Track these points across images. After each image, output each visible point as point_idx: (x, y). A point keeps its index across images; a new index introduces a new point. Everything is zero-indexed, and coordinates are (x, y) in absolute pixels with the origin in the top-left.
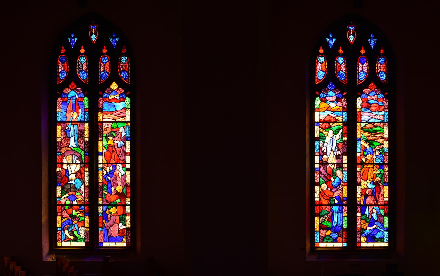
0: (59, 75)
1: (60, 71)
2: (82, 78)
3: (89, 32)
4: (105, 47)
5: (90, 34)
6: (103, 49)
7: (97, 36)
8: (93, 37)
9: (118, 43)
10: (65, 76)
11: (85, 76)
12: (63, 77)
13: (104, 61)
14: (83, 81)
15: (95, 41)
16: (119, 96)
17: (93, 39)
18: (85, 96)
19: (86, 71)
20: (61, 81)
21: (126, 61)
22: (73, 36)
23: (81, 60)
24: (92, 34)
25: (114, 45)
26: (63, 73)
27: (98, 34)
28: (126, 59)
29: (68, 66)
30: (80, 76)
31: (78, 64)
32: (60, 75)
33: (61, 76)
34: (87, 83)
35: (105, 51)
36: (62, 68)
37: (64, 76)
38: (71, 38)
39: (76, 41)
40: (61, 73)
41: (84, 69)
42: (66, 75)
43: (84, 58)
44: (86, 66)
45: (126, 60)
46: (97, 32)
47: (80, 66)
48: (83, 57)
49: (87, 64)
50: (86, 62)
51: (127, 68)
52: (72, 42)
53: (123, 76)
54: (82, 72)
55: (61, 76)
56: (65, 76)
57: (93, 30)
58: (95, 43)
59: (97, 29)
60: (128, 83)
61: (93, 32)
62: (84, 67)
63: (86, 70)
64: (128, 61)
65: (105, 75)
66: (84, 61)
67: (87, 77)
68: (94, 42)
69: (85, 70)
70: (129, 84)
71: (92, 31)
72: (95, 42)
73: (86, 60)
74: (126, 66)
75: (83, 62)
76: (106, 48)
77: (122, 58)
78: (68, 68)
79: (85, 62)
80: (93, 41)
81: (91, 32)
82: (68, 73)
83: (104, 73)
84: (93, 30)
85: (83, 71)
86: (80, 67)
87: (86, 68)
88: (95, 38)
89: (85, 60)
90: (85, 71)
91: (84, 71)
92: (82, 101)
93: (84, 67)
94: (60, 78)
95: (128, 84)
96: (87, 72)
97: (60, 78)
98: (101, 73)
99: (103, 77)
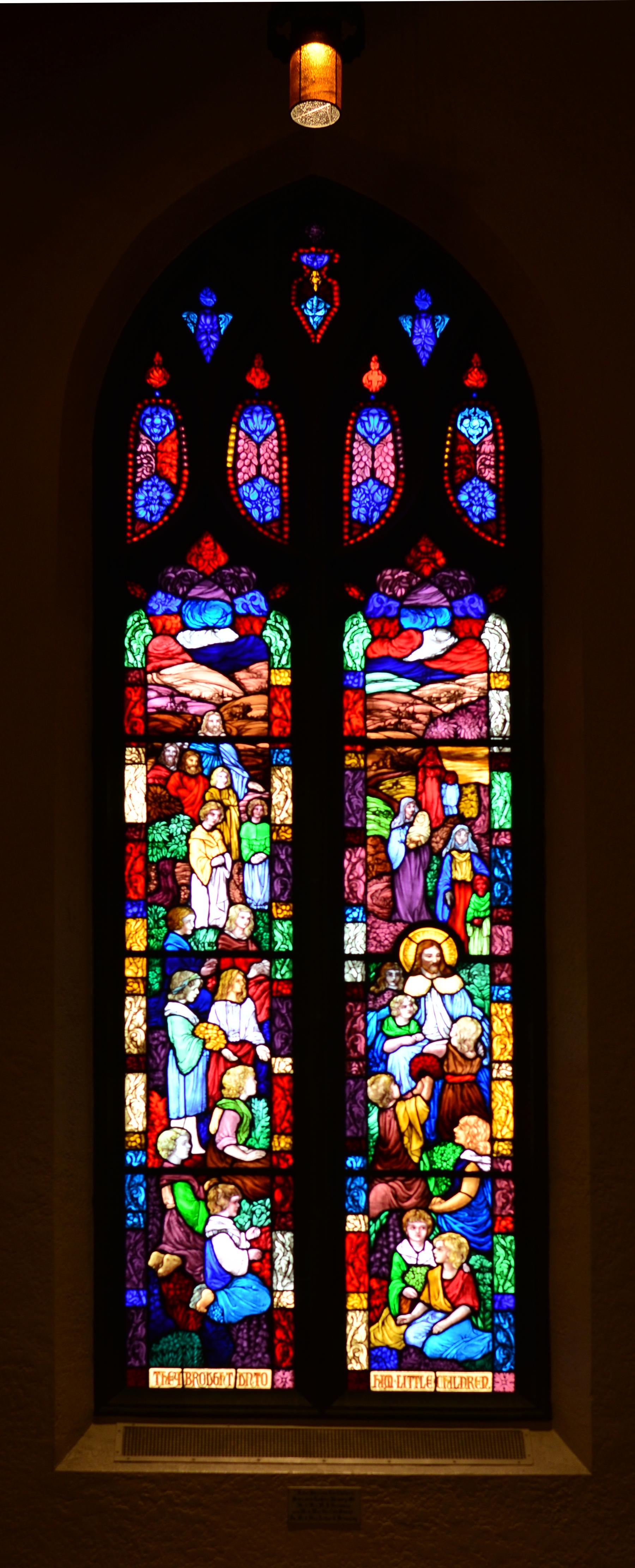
0: (135, 499)
1: (143, 480)
2: (255, 513)
6: (368, 369)
7: (332, 306)
9: (441, 343)
10: (169, 507)
11: (272, 505)
12: (154, 508)
14: (266, 533)
15: (322, 332)
16: (451, 609)
19: (277, 481)
21: (486, 432)
22: (210, 301)
23: (247, 424)
27: (336, 293)
28: (482, 418)
29: (181, 454)
30: (248, 504)
31: (236, 446)
35: (374, 379)
36: (153, 463)
37: (160, 504)
38: (201, 310)
39: (223, 327)
40: (148, 491)
41: (264, 470)
42: (173, 500)
43: (264, 413)
44: (273, 456)
45: (483, 428)
46: (336, 288)
47: (243, 456)
48: (258, 408)
49: (279, 446)
50: (275, 434)
51: (489, 466)
54: (256, 485)
56: (167, 502)
58: (321, 340)
60: (495, 542)
62: (266, 462)
63: (277, 475)
64: (494, 431)
66: (263, 427)
67: (279, 508)
68: (316, 338)
69: (271, 477)
70: (502, 545)
72: (323, 336)
73: (273, 424)
74: (486, 459)
75: (262, 431)
76: (383, 369)
77: (465, 417)
78: (180, 468)
79: (270, 434)
80: (311, 327)
85: (261, 480)
86: (246, 458)
87: (277, 463)
89: (268, 424)
90: (271, 482)
91: (266, 479)
93: (266, 462)
95: (497, 546)
96: (280, 485)
97: (142, 513)
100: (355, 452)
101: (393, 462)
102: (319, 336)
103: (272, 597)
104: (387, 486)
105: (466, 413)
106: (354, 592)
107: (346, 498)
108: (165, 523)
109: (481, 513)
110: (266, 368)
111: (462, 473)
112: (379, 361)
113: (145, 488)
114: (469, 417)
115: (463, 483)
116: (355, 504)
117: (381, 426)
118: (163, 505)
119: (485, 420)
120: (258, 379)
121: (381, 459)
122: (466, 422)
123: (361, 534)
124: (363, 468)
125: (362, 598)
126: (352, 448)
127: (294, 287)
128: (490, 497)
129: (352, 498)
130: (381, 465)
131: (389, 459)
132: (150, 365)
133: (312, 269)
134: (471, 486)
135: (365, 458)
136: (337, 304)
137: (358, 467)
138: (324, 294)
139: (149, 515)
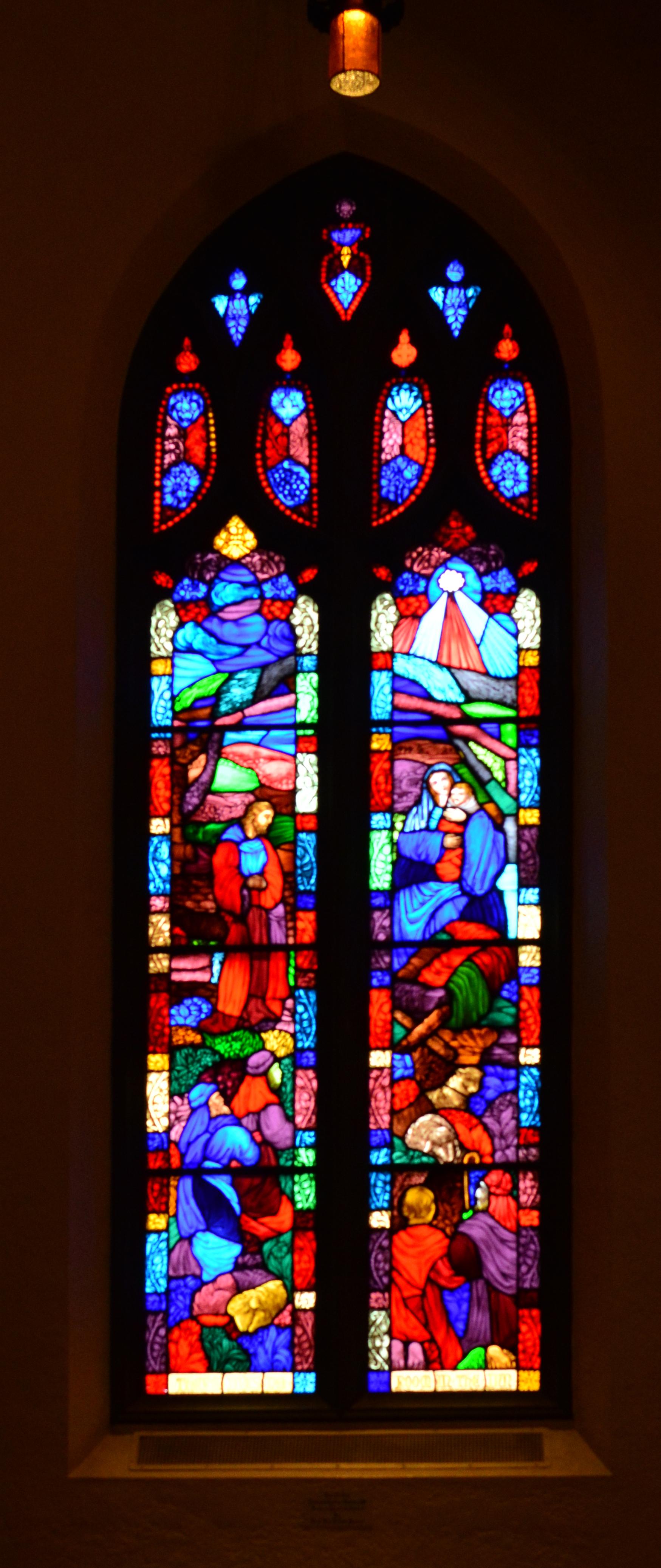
4: (404, 337)
7: (363, 281)
8: (343, 288)
12: (182, 494)
17: (346, 298)
18: (301, 590)
20: (171, 518)
24: (336, 270)
25: (455, 319)
26: (183, 475)
28: (514, 389)
32: (169, 484)
33: (173, 493)
37: (188, 490)
45: (514, 399)
52: (234, 318)
53: (504, 479)
55: (173, 493)
57: (346, 250)
61: (346, 260)
71: (339, 255)
76: (413, 342)
77: (496, 390)
81: (331, 262)
82: (210, 478)
84: (346, 250)
88: (355, 289)
92: (283, 616)
94: (169, 499)
100: (385, 429)
101: (423, 437)
102: (350, 312)
103: (301, 581)
104: (416, 462)
105: (497, 385)
107: (375, 477)
109: (513, 488)
110: (296, 348)
111: (492, 448)
112: (410, 335)
113: (173, 474)
114: (501, 389)
115: (495, 456)
116: (384, 482)
117: (412, 399)
119: (517, 391)
120: (290, 359)
121: (412, 435)
122: (498, 394)
123: (389, 512)
124: (393, 446)
125: (390, 579)
126: (382, 425)
128: (522, 469)
129: (381, 477)
130: (411, 442)
131: (420, 434)
132: (178, 349)
133: (342, 245)
134: (503, 460)
135: (394, 436)
137: (388, 445)
138: (355, 269)
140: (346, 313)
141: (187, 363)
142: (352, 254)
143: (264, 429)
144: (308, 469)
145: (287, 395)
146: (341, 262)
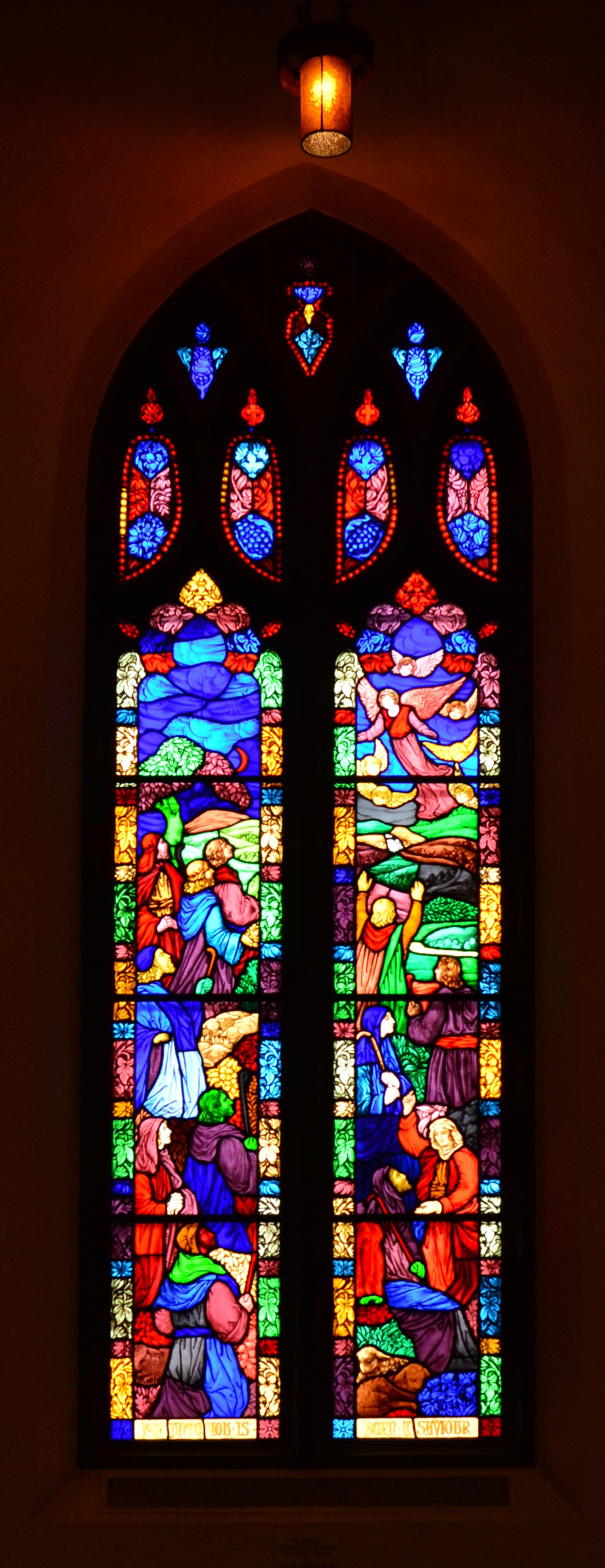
0: (128, 535)
3: (288, 317)
5: (292, 330)
13: (361, 461)
24: (300, 326)
34: (279, 580)
35: (368, 413)
40: (141, 528)
58: (317, 372)
59: (324, 307)
65: (366, 536)
70: (494, 579)
81: (295, 320)
82: (175, 529)
83: (361, 527)
95: (489, 581)
98: (346, 522)
99: (358, 544)
102: (314, 368)
106: (345, 630)
108: (158, 562)
118: (155, 542)
120: (253, 412)
127: (289, 320)
136: (331, 337)
139: (141, 552)
140: (310, 370)
141: (151, 412)
142: (315, 311)
143: (229, 483)
144: (273, 524)
145: (251, 449)
146: (305, 320)
